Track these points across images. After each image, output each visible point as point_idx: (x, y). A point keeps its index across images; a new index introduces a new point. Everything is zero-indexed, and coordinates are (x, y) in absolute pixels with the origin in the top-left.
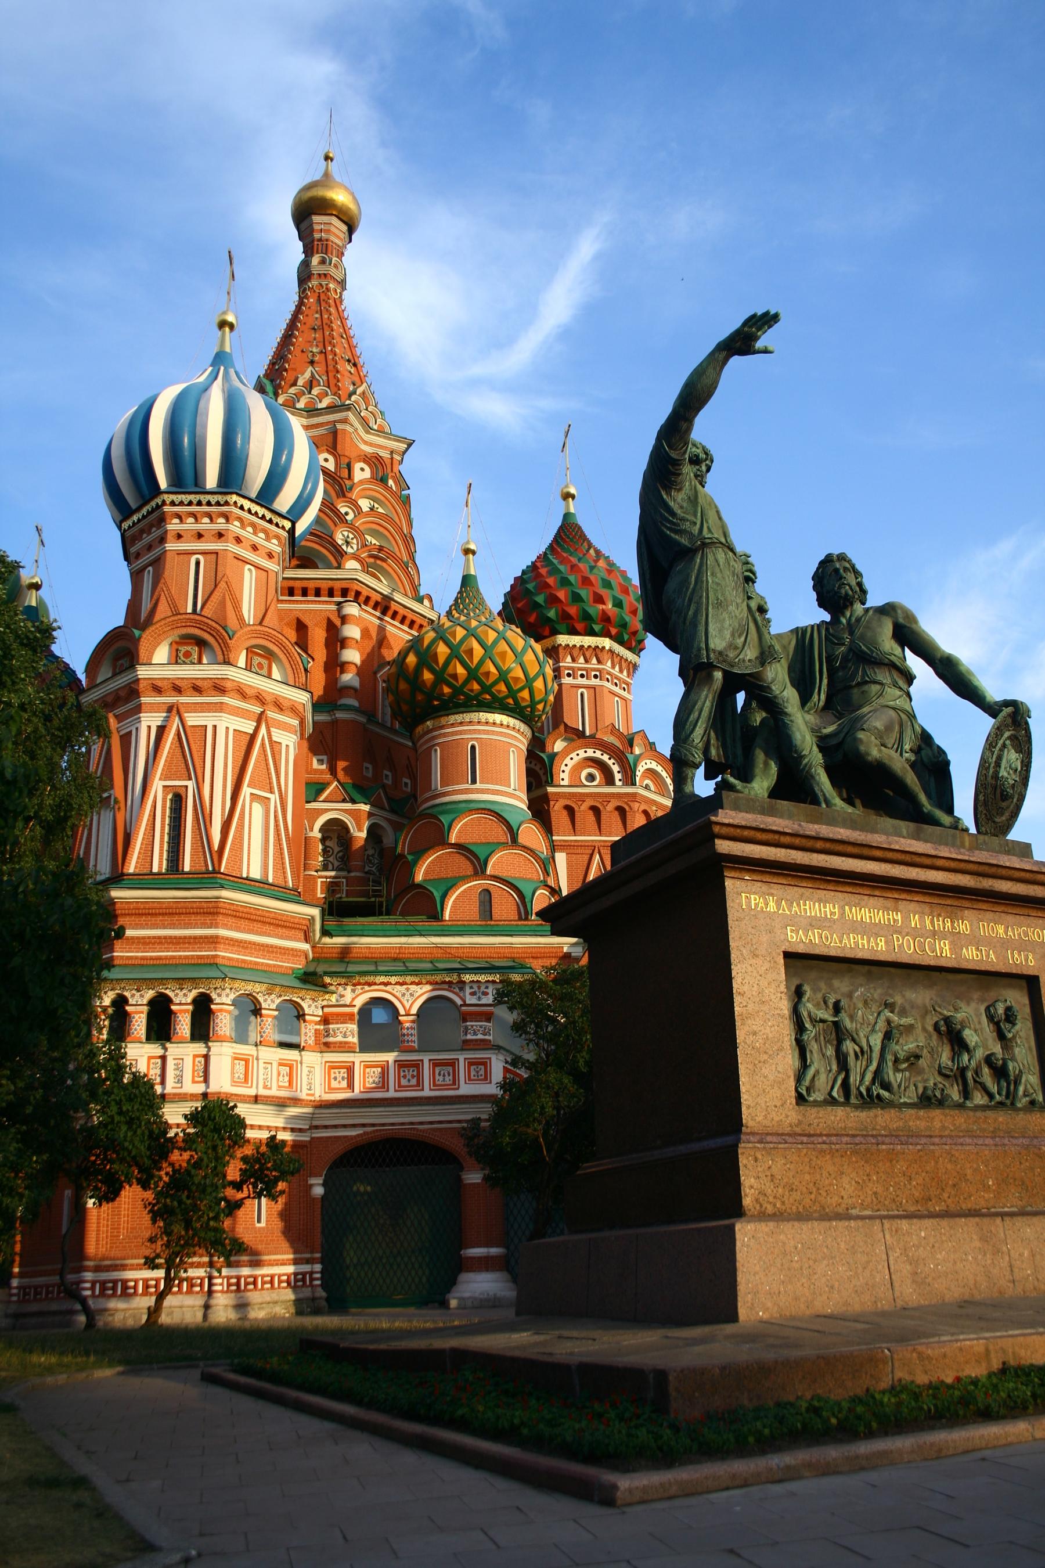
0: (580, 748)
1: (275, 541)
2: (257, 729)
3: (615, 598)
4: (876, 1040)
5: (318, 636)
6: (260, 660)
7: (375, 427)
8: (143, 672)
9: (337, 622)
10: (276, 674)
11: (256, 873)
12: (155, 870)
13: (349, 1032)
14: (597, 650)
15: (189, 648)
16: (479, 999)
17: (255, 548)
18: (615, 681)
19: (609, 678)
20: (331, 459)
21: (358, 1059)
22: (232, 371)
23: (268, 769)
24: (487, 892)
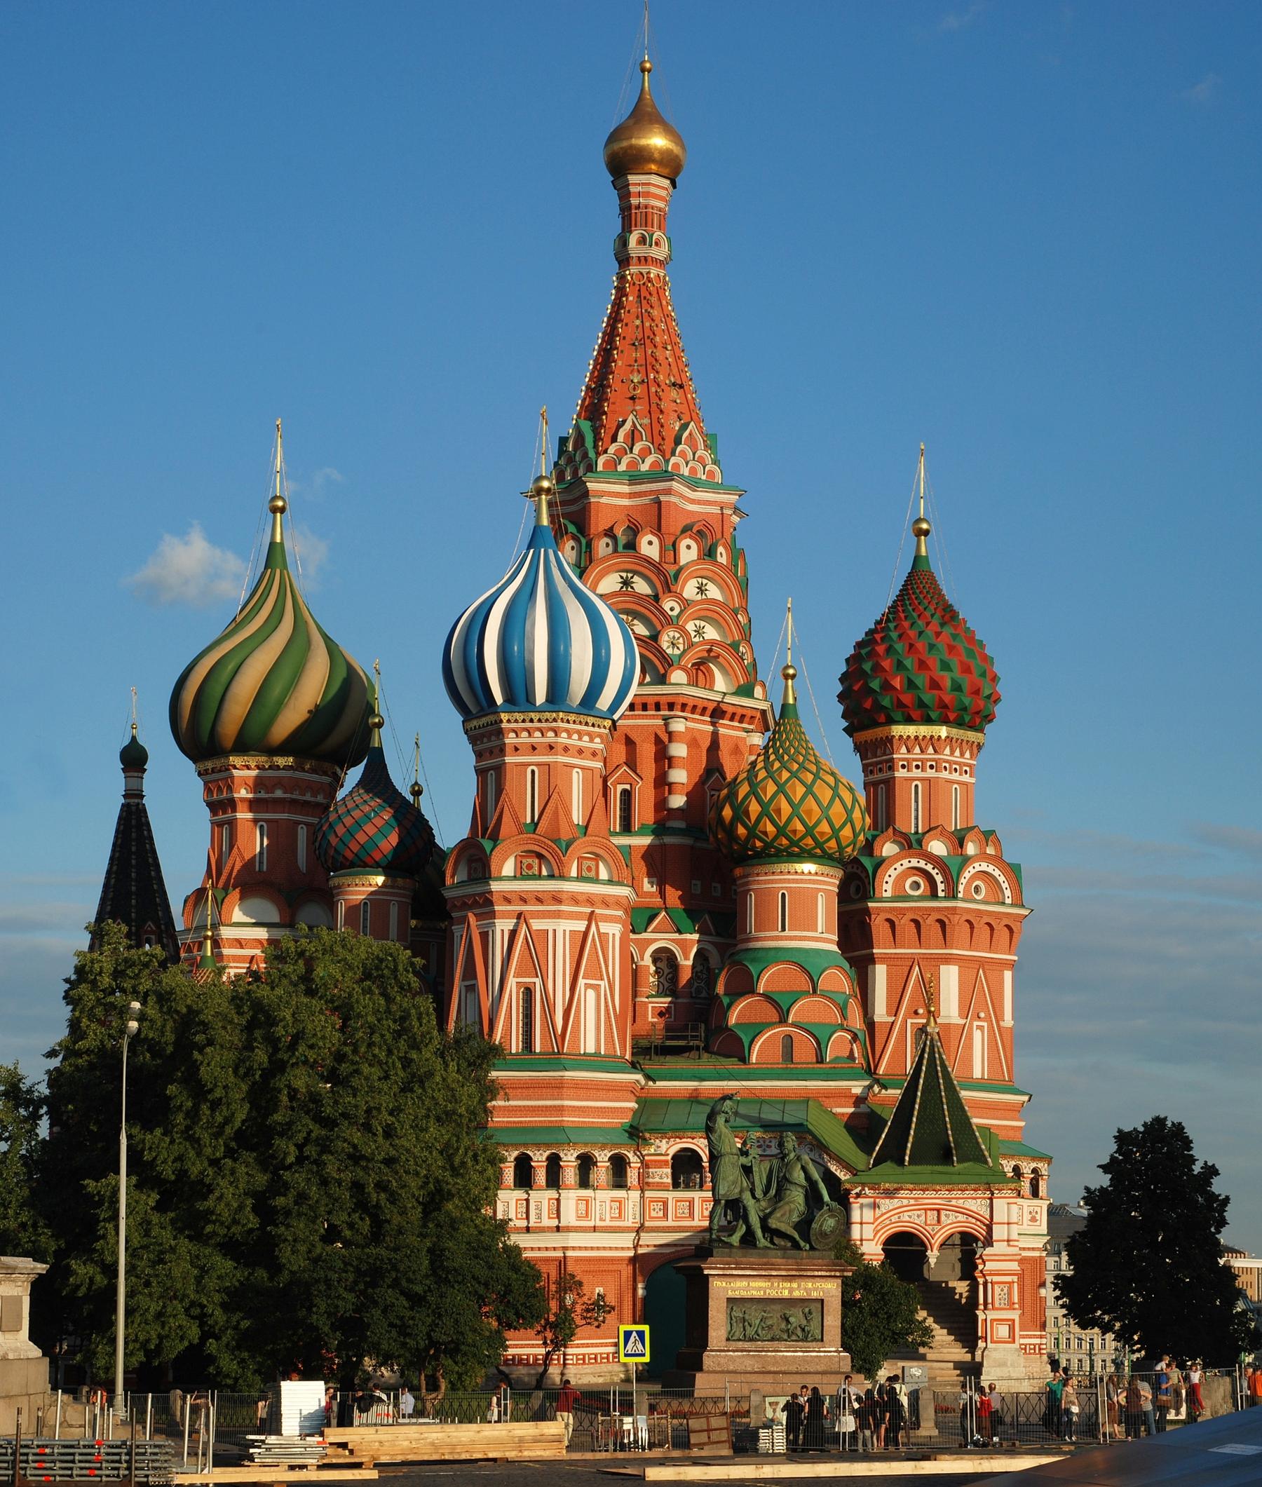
1: (598, 740)
2: (588, 927)
3: (962, 663)
4: (757, 1322)
5: (647, 751)
7: (704, 477)
8: (495, 886)
9: (665, 738)
10: (604, 875)
11: (591, 1049)
12: (514, 1051)
13: (664, 1175)
14: (933, 741)
15: (530, 861)
16: (764, 1150)
18: (954, 766)
19: (947, 765)
20: (655, 540)
21: (671, 1195)
22: (551, 552)
23: (599, 960)
24: (789, 1038)
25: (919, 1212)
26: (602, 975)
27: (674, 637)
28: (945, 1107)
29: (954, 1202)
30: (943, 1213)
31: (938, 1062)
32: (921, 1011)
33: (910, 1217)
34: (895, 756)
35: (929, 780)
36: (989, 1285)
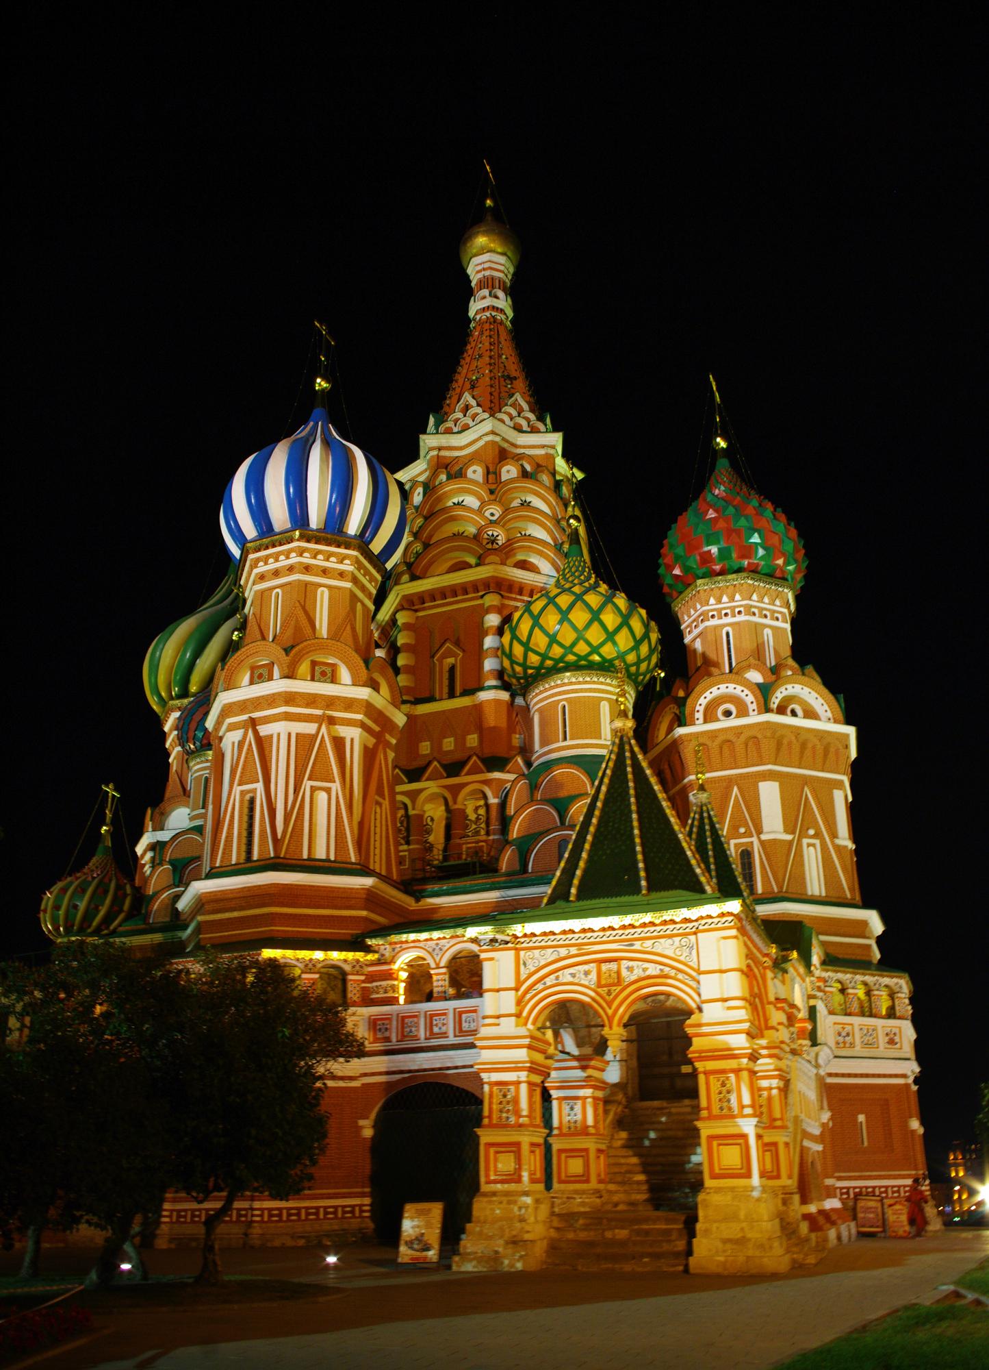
0: (711, 687)
1: (347, 561)
6: (324, 668)
7: (529, 430)
11: (320, 853)
12: (233, 862)
15: (261, 671)
17: (325, 572)
25: (586, 967)
26: (334, 777)
27: (493, 535)
28: (634, 816)
29: (638, 945)
30: (625, 964)
31: (628, 762)
32: (742, 830)
33: (573, 975)
34: (704, 608)
35: (738, 623)
36: (702, 1078)
